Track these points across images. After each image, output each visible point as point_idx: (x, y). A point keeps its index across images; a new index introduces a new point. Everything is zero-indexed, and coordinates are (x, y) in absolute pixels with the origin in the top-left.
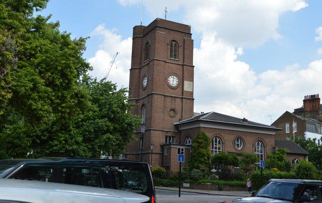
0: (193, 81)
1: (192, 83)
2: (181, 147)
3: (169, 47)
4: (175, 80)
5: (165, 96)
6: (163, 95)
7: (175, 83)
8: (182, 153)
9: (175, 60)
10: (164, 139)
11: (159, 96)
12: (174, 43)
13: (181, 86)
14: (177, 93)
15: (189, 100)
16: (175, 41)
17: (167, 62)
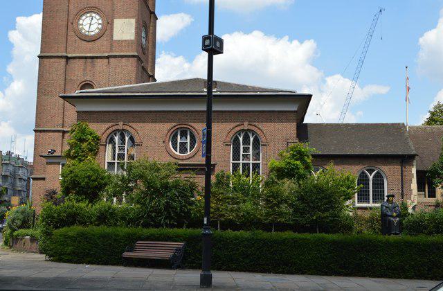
4: (95, 21)
5: (67, 58)
6: (61, 57)
14: (100, 49)
15: (124, 60)
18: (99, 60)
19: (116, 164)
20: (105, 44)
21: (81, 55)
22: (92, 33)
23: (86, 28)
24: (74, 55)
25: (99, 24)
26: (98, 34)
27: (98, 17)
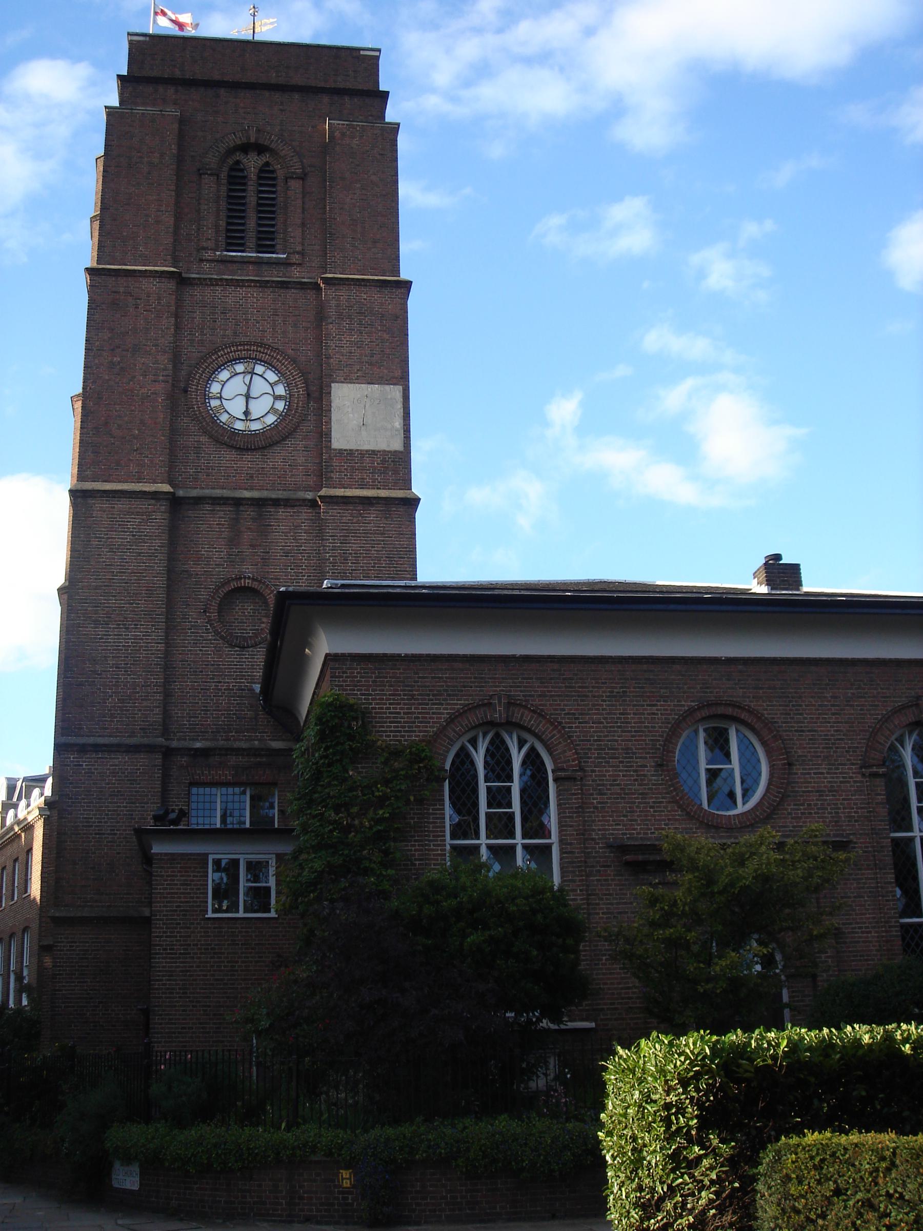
0: (402, 378)
1: (396, 392)
2: (244, 853)
4: (259, 386)
7: (259, 407)
8: (260, 897)
9: (258, 263)
11: (121, 505)
12: (252, 163)
15: (372, 515)
16: (261, 149)
17: (202, 282)
18: (282, 512)
19: (519, 850)
20: (301, 460)
21: (218, 492)
22: (255, 426)
23: (236, 407)
24: (194, 493)
25: (277, 398)
26: (275, 427)
27: (272, 376)
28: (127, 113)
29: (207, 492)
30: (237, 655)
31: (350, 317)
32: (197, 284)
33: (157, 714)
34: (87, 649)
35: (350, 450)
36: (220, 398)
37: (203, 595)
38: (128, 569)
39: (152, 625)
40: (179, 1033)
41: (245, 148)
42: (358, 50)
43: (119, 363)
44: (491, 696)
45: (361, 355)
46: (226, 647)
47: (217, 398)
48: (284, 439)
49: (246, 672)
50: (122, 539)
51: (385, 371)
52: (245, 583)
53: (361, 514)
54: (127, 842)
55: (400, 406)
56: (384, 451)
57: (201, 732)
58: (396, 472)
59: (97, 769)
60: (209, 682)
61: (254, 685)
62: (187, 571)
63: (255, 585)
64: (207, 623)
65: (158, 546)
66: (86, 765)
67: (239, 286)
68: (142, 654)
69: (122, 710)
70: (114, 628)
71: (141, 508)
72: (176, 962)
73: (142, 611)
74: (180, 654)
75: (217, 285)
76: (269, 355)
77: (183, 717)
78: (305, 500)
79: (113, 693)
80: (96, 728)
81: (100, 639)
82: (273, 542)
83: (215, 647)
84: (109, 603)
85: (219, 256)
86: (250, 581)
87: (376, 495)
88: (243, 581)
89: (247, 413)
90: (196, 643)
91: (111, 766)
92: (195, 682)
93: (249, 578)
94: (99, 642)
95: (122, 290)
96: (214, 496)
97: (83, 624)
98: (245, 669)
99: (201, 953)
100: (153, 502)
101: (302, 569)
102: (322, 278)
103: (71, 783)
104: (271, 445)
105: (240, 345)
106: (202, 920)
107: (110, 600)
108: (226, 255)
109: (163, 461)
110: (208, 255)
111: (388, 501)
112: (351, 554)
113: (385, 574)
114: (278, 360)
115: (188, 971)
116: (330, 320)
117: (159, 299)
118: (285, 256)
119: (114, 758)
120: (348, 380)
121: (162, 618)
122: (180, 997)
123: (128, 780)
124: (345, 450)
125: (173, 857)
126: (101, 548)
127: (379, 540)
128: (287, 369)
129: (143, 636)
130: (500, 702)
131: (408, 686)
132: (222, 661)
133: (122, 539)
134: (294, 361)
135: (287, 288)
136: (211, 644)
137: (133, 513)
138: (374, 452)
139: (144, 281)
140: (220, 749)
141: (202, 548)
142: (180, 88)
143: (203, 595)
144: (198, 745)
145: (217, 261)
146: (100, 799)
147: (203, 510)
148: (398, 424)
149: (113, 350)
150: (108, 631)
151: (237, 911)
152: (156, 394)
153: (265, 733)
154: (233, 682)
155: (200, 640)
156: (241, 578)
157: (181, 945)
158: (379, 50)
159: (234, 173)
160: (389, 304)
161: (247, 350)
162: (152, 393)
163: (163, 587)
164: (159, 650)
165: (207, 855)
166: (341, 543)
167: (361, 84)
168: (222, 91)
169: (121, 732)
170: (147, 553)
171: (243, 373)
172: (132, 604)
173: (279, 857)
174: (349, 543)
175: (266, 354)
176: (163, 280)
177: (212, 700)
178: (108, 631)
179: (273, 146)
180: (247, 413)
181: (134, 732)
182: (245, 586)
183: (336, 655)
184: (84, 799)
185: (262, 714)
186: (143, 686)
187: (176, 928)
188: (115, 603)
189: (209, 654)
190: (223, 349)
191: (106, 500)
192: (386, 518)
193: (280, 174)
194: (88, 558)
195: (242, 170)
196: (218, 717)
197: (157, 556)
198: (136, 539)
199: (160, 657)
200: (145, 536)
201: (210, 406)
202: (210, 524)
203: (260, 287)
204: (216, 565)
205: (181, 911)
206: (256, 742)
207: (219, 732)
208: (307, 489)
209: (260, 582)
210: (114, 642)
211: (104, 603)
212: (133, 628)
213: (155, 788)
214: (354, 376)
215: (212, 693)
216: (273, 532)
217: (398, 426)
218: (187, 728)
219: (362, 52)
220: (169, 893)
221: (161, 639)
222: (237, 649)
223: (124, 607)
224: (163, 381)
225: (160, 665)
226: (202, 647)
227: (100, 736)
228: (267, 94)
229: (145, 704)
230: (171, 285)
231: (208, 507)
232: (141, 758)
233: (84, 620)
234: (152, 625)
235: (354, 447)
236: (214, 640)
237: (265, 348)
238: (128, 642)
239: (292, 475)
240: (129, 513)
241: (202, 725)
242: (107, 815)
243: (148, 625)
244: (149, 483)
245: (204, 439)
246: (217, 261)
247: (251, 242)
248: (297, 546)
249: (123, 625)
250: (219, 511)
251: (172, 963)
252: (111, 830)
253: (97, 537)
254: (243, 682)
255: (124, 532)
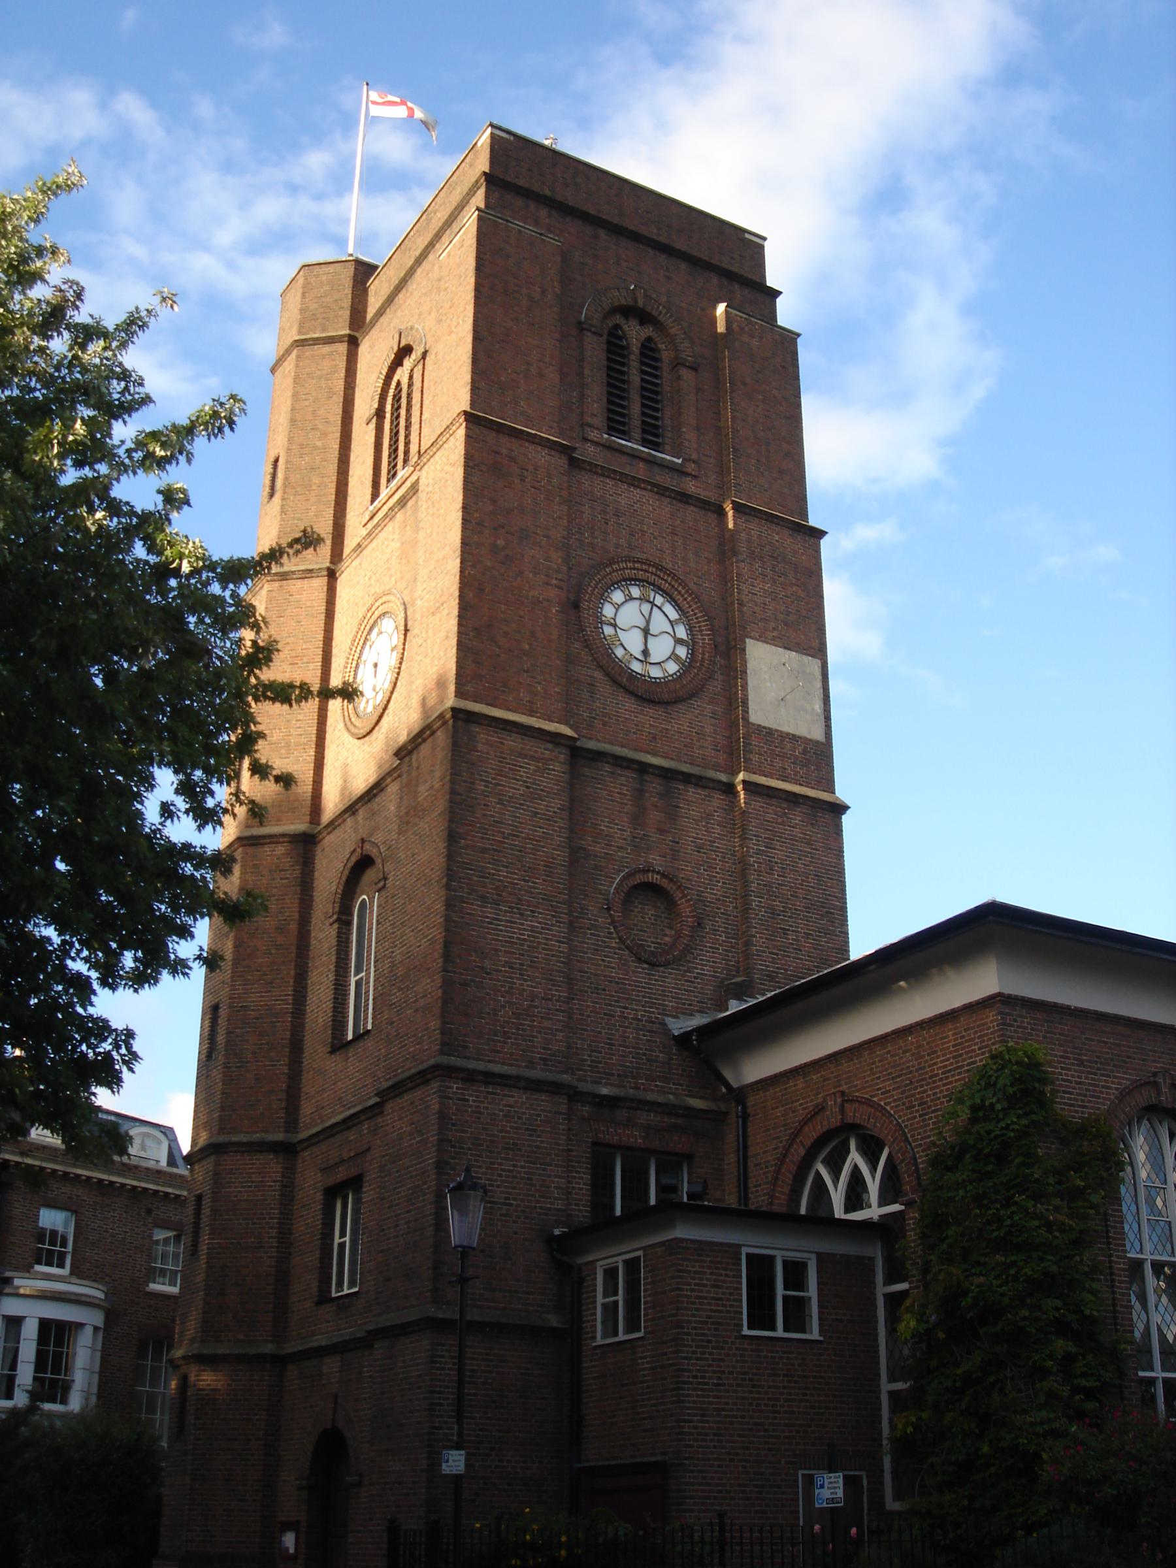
0: (818, 650)
1: (814, 665)
3: (595, 350)
7: (661, 648)
8: (796, 1314)
10: (582, 1182)
11: (512, 742)
12: (635, 333)
13: (716, 686)
15: (797, 817)
16: (645, 318)
18: (692, 793)
20: (709, 729)
22: (656, 673)
23: (632, 642)
24: (592, 745)
25: (679, 641)
27: (673, 614)
28: (501, 224)
29: (605, 747)
30: (646, 974)
31: (761, 558)
32: (586, 470)
33: (561, 1041)
34: (472, 935)
35: (770, 729)
36: (615, 626)
37: (604, 885)
38: (522, 832)
39: (553, 916)
40: (715, 1498)
41: (628, 311)
42: (744, 231)
43: (504, 548)
44: (1155, 1074)
45: (776, 610)
46: (633, 961)
47: (611, 624)
48: (690, 698)
49: (656, 999)
50: (515, 789)
51: (802, 637)
52: (652, 877)
53: (786, 813)
54: (526, 1218)
55: (819, 684)
56: (805, 738)
57: (605, 1073)
58: (818, 769)
59: (487, 1108)
60: (613, 1006)
61: (666, 1018)
62: (585, 849)
63: (664, 883)
64: (609, 924)
65: (559, 809)
66: (474, 1101)
67: (633, 485)
68: (540, 953)
69: (518, 1029)
70: (506, 911)
71: (536, 751)
72: (708, 1397)
73: (540, 894)
74: (579, 961)
75: (608, 477)
76: (670, 584)
77: (584, 1050)
78: (720, 782)
79: (508, 1002)
80: (484, 1050)
81: (489, 923)
82: (683, 830)
83: (620, 959)
84: (499, 876)
85: (606, 439)
86: (659, 877)
87: (802, 793)
88: (650, 874)
89: (646, 652)
90: (597, 950)
91: (505, 1106)
92: (597, 1003)
93: (658, 873)
94: (488, 928)
95: (504, 451)
96: (617, 754)
97: (467, 898)
98: (654, 994)
99: (738, 1385)
100: (550, 746)
101: (717, 872)
102: (733, 502)
103: (454, 1125)
104: (675, 702)
105: (638, 562)
106: (736, 1337)
107: (501, 871)
108: (615, 442)
109: (558, 693)
110: (593, 435)
111: (794, 799)
112: (776, 863)
113: (814, 896)
114: (680, 592)
115: (723, 1410)
116: (741, 557)
117: (549, 476)
118: (680, 461)
119: (508, 1096)
120: (762, 638)
121: (564, 909)
122: (715, 1447)
123: (527, 1129)
124: (764, 728)
125: (701, 1247)
126: (488, 796)
127: (805, 852)
128: (690, 606)
129: (542, 928)
130: (1165, 1083)
131: (1076, 1048)
132: (627, 980)
133: (515, 789)
134: (697, 598)
135: (687, 503)
136: (615, 953)
137: (526, 756)
138: (794, 738)
139: (531, 447)
140: (632, 1100)
141: (602, 821)
142: (553, 212)
143: (604, 885)
144: (605, 1091)
145: (603, 445)
146: (490, 1152)
147: (601, 770)
148: (818, 707)
149: (495, 528)
150: (498, 915)
151: (773, 1328)
152: (548, 601)
153: (681, 1085)
154: (641, 1010)
155: (601, 946)
156: (648, 871)
157: (714, 1372)
158: (765, 239)
159: (613, 340)
160: (803, 554)
161: (645, 571)
162: (544, 599)
163: (563, 866)
164: (561, 952)
165: (739, 1246)
166: (766, 847)
167: (745, 271)
168: (602, 233)
169: (516, 1060)
170: (544, 814)
171: (640, 599)
172: (527, 881)
173: (820, 1257)
174: (775, 849)
175: (666, 581)
176: (553, 453)
177: (617, 1030)
178: (498, 915)
179: (662, 318)
180: (646, 652)
181: (532, 1063)
182: (652, 883)
183: (1009, 997)
184: (470, 1149)
185: (676, 1059)
186: (543, 999)
187: (707, 1347)
188: (507, 877)
189: (613, 968)
190: (618, 562)
191: (494, 732)
192: (812, 824)
193: (666, 355)
194: (472, 807)
195: (620, 338)
196: (624, 1056)
197: (556, 822)
198: (531, 793)
199: (562, 962)
200: (542, 790)
201: (603, 633)
202: (610, 791)
203: (657, 493)
204: (618, 847)
205: (712, 1323)
206: (671, 1097)
207: (626, 1077)
208: (716, 768)
209: (671, 880)
210: (506, 931)
211: (494, 874)
212: (529, 916)
213: (559, 1145)
214: (770, 635)
215: (617, 1021)
216: (682, 817)
217: (819, 711)
218: (589, 1066)
219: (747, 236)
220: (696, 1297)
221: (564, 937)
222: (645, 966)
223: (517, 884)
224: (556, 586)
225: (562, 972)
226: (605, 956)
227: (489, 1061)
228: (651, 252)
229: (547, 1024)
230: (561, 462)
231: (607, 768)
232: (542, 1101)
233: (468, 893)
234: (553, 916)
235: (774, 726)
236: (620, 949)
237: (665, 573)
238: (524, 935)
239: (700, 746)
240: (521, 755)
241: (606, 1063)
242: (500, 1175)
243: (547, 915)
244: (545, 719)
245: (598, 675)
246: (603, 445)
247: (637, 433)
248: (710, 841)
249: (518, 909)
250: (622, 775)
251: (703, 1396)
252: (506, 1198)
253: (483, 781)
254: (653, 1012)
255: (515, 779)
